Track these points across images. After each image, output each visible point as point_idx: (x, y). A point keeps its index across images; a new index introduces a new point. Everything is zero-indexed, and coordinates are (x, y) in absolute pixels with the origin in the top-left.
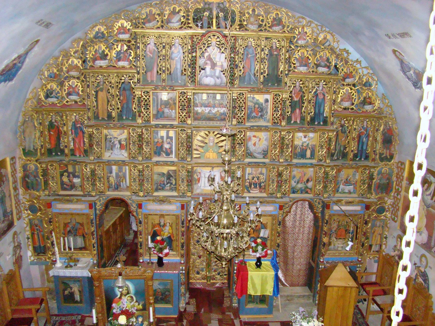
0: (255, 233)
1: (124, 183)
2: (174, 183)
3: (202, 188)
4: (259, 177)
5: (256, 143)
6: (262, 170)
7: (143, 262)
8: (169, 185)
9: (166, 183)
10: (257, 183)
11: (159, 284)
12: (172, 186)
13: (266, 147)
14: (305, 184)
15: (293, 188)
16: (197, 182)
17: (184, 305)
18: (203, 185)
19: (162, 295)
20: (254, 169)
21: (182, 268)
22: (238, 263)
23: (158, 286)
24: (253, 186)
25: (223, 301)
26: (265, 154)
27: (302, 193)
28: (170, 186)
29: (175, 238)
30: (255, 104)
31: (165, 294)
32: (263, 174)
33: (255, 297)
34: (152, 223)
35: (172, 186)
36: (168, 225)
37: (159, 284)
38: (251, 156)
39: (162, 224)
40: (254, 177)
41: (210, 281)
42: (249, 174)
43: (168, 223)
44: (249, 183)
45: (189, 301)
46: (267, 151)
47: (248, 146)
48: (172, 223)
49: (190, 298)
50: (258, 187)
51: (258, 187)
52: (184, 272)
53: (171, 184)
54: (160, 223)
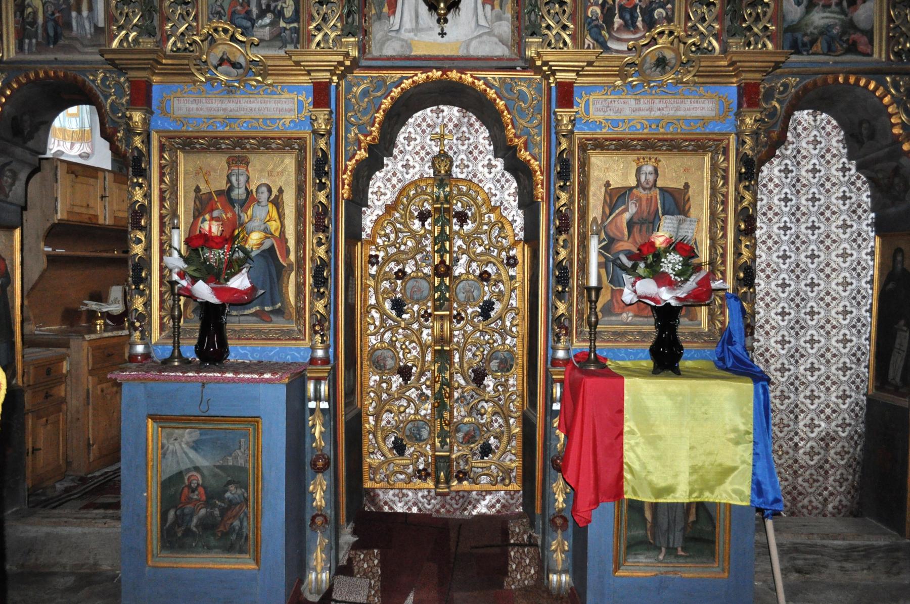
0: (636, 229)
1: (85, 13)
2: (288, 13)
3: (405, 35)
7: (147, 356)
8: (267, 20)
9: (255, 11)
10: (635, 6)
11: (196, 446)
12: (282, 24)
14: (843, 12)
15: (792, 29)
16: (386, 10)
17: (325, 576)
18: (408, 24)
19: (208, 503)
21: (317, 390)
22: (567, 362)
23: (192, 454)
24: (617, 21)
25: (507, 564)
27: (830, 51)
28: (273, 24)
29: (292, 257)
31: (220, 495)
33: (663, 521)
34: (197, 190)
35: (282, 24)
36: (264, 196)
37: (196, 446)
39: (239, 193)
41: (447, 482)
43: (264, 189)
44: (602, 6)
45: (350, 560)
48: (281, 191)
49: (355, 547)
50: (639, 24)
51: (639, 24)
52: (324, 405)
53: (279, 14)
54: (231, 189)
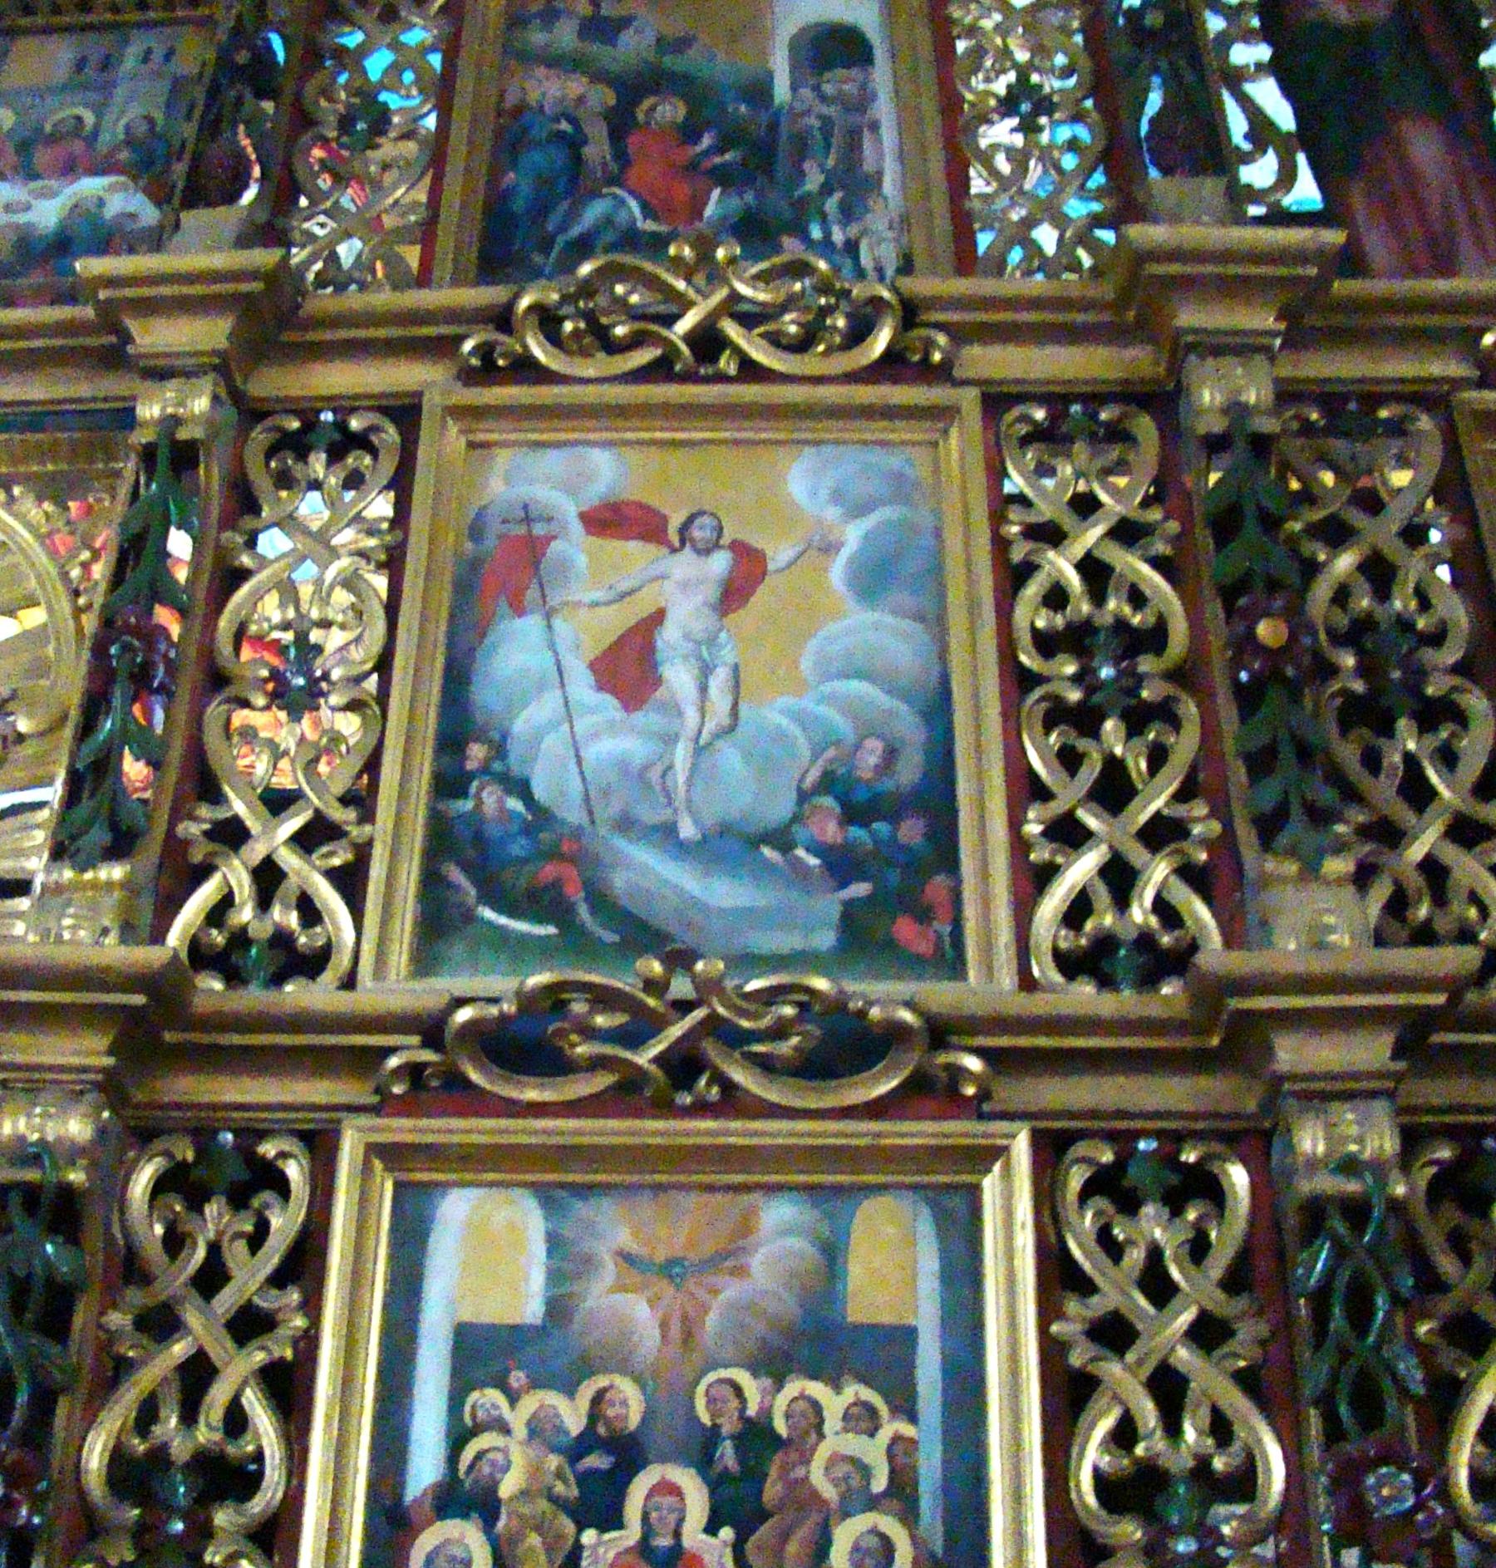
4: (757, 1436)
5: (669, 635)
6: (832, 1254)
13: (908, 725)
20: (614, 1227)
26: (885, 844)
30: (634, 88)
32: (882, 1357)
38: (542, 902)
40: (629, 1454)
42: (481, 1354)
46: (936, 800)
47: (485, 695)
